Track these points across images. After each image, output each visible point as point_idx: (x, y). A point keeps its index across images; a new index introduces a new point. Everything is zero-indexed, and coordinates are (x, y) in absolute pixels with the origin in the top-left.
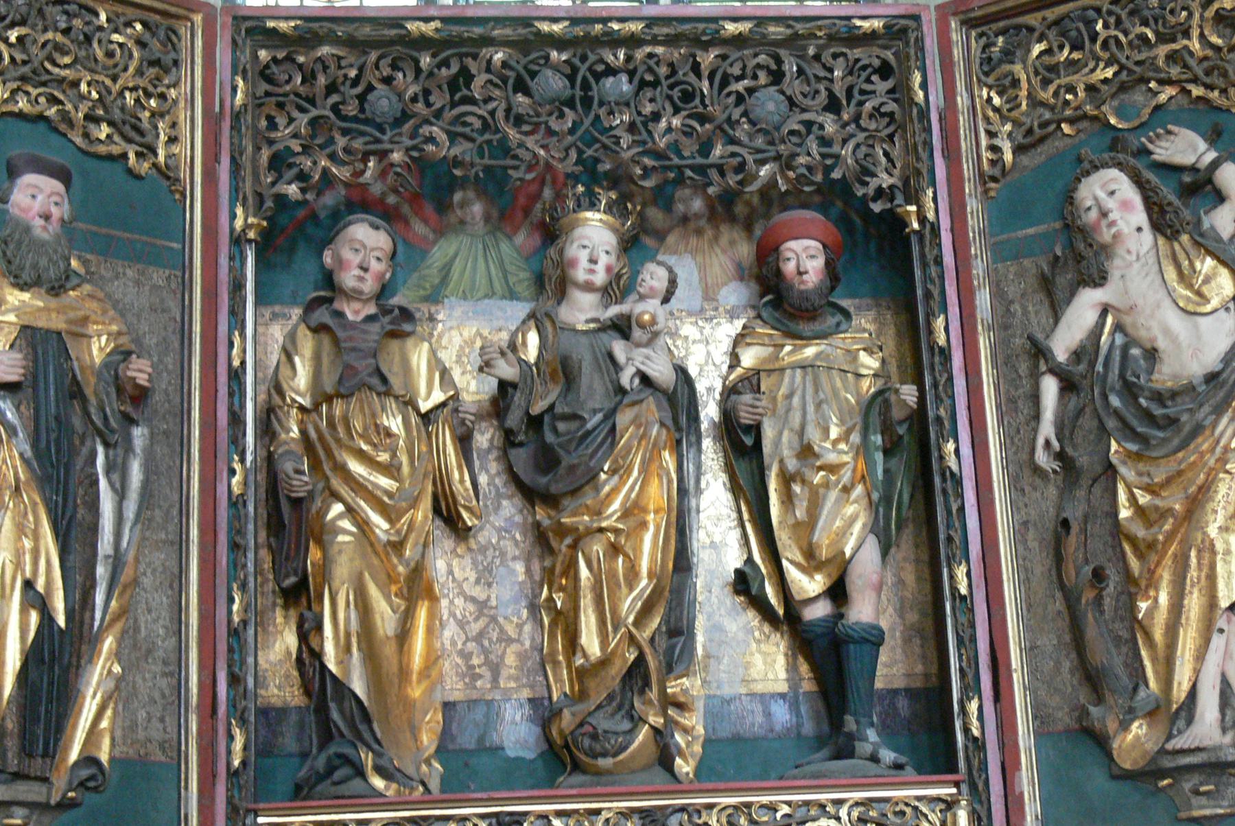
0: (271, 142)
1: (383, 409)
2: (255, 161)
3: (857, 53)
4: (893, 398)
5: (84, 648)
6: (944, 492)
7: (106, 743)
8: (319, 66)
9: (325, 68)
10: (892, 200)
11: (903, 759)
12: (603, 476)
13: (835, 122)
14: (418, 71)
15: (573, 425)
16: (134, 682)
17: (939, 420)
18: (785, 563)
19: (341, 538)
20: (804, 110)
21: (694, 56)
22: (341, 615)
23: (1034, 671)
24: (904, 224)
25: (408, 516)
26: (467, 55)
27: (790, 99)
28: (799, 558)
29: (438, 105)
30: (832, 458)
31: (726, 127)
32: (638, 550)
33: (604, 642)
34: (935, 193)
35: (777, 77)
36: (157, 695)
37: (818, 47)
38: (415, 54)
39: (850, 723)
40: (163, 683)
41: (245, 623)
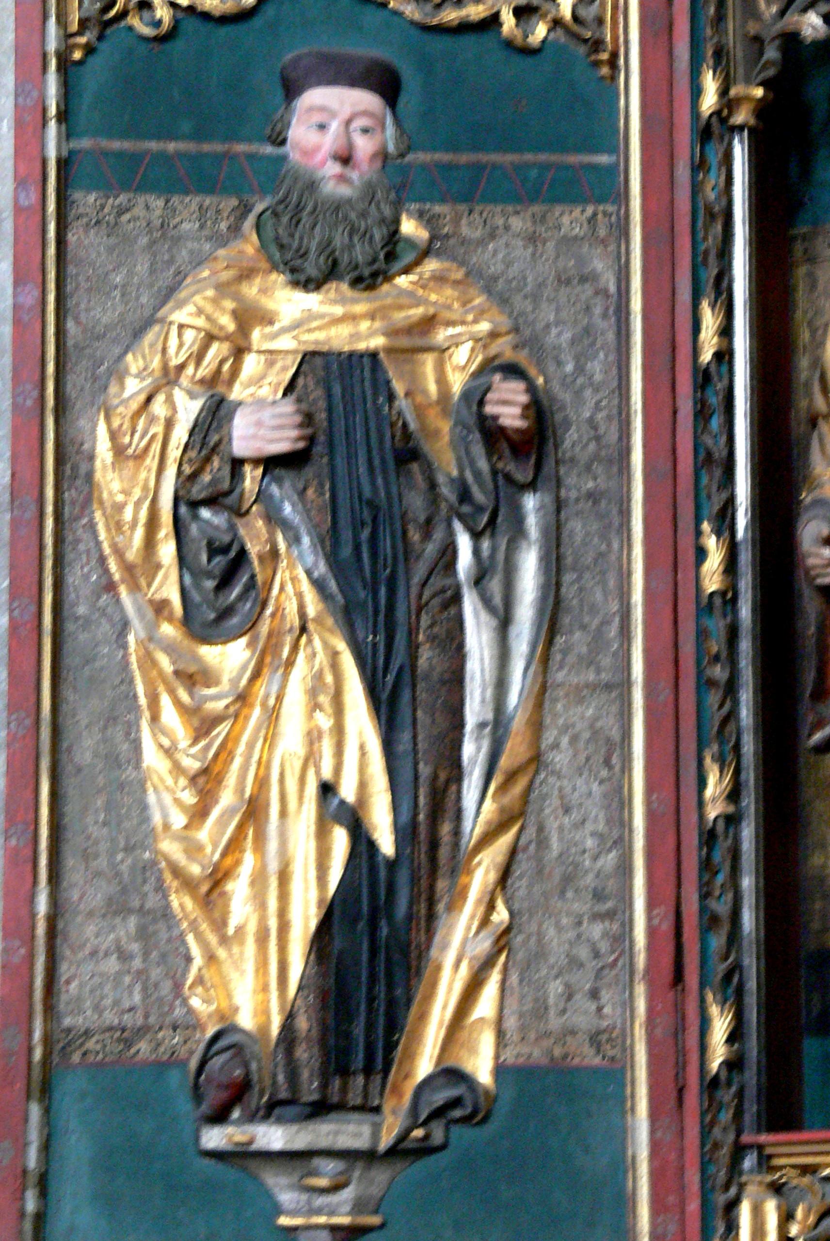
5: (441, 885)
7: (487, 1042)
16: (540, 935)
36: (583, 953)
40: (596, 930)
41: (732, 820)
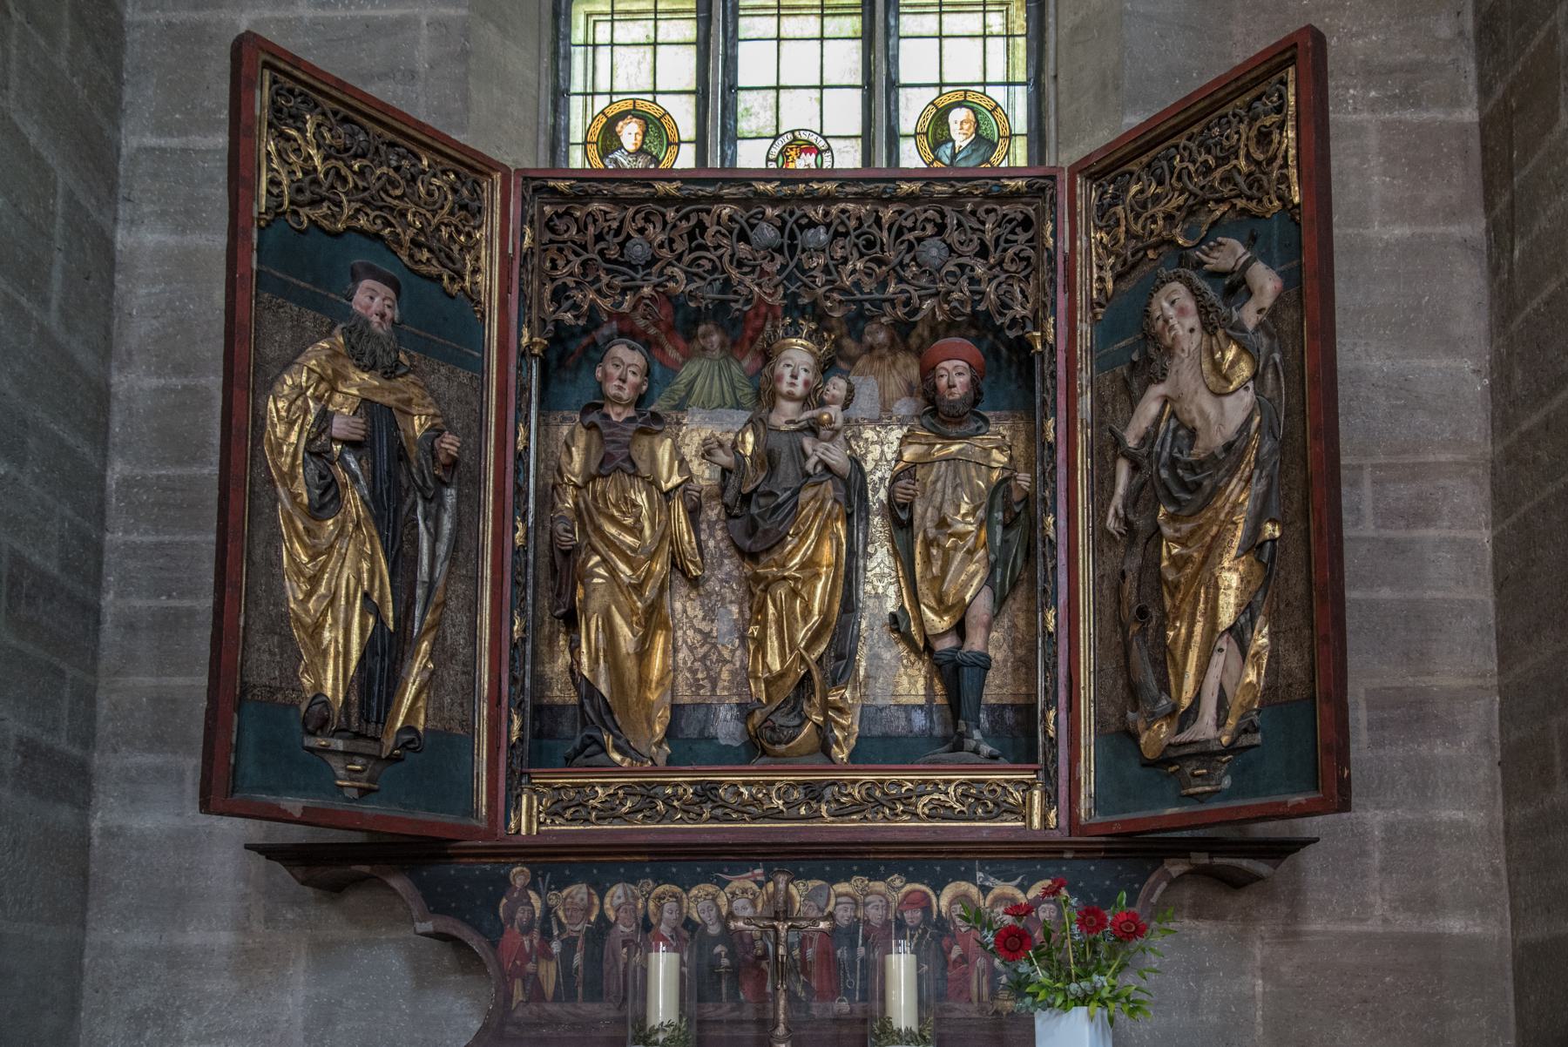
0: (553, 280)
1: (632, 486)
2: (540, 294)
3: (1006, 209)
4: (1013, 483)
6: (1044, 554)
8: (590, 220)
9: (595, 221)
10: (1023, 328)
11: (997, 752)
12: (789, 539)
13: (984, 265)
14: (665, 223)
15: (770, 500)
17: (1044, 499)
18: (922, 606)
19: (596, 580)
20: (960, 256)
21: (877, 212)
22: (593, 636)
23: (1098, 689)
24: (1031, 347)
25: (646, 565)
26: (702, 210)
27: (949, 246)
28: (933, 604)
29: (679, 251)
30: (960, 527)
31: (898, 268)
32: (812, 594)
33: (783, 662)
34: (1055, 321)
35: (941, 229)
36: (458, 688)
37: (974, 204)
38: (663, 210)
39: (962, 727)
41: (524, 640)
